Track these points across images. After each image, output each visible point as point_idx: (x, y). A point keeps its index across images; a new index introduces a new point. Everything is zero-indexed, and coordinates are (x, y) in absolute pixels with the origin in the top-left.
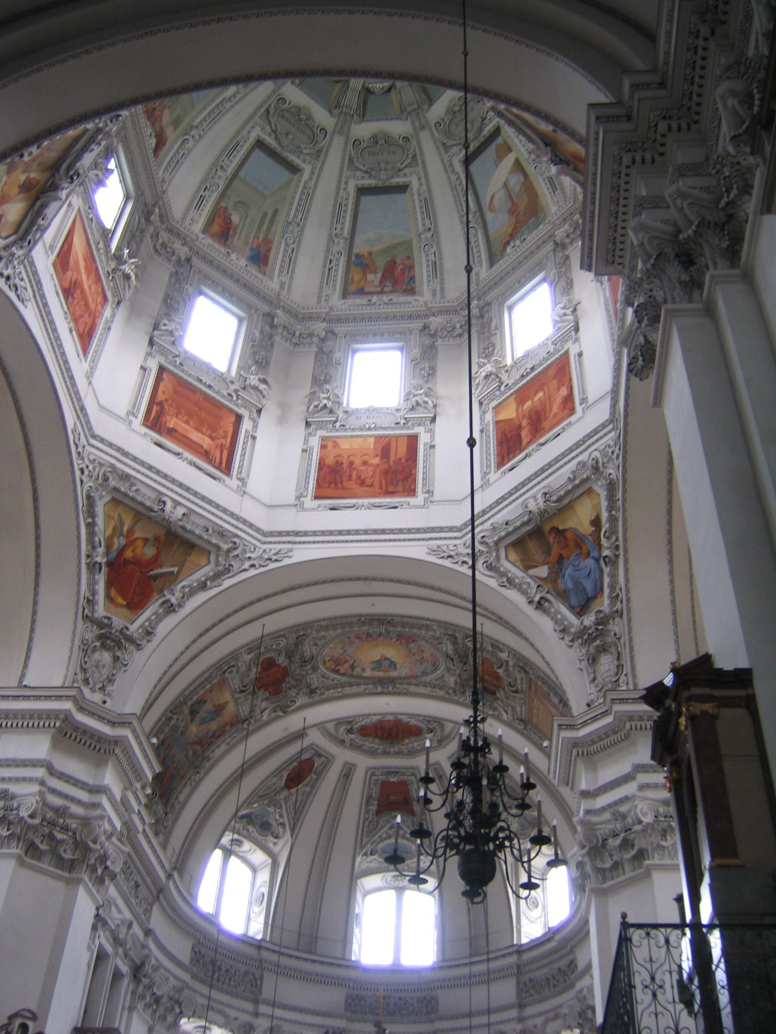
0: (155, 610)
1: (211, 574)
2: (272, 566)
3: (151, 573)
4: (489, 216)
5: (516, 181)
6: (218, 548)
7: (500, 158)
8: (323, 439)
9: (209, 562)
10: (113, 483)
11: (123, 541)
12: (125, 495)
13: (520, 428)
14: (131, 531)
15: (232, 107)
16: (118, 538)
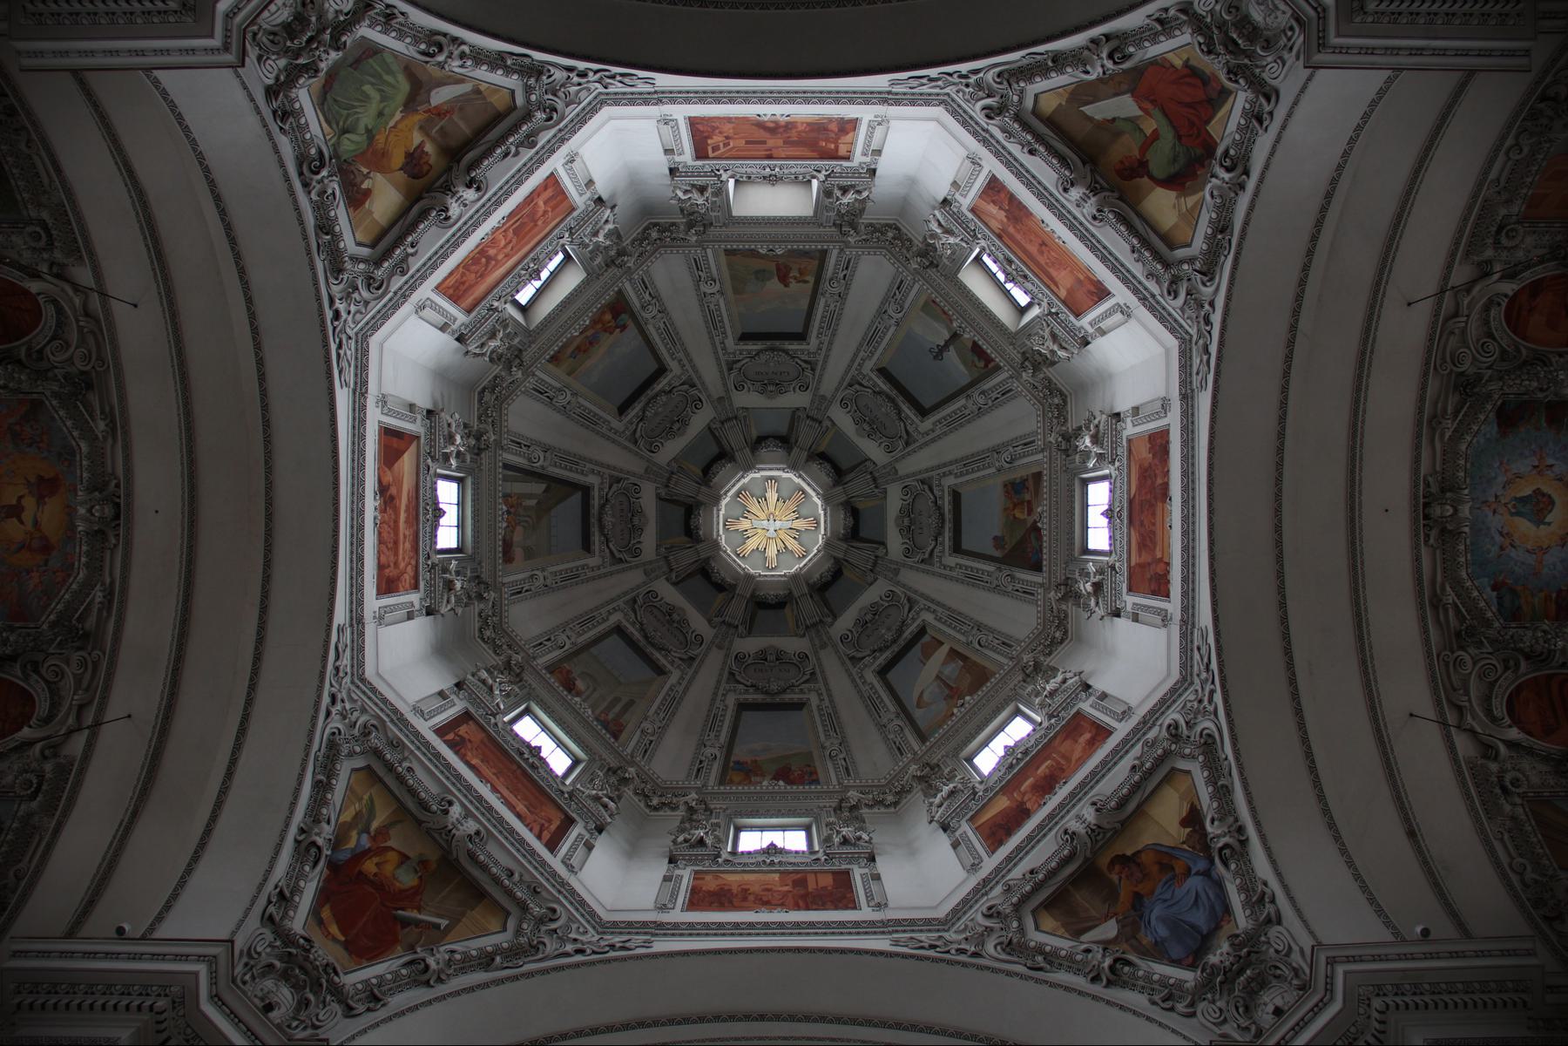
0: (394, 968)
1: (505, 945)
2: (612, 954)
3: (400, 912)
4: (918, 714)
5: (953, 670)
6: (523, 907)
7: (927, 654)
8: (696, 872)
9: (505, 929)
10: (375, 740)
11: (366, 842)
12: (390, 768)
13: (1022, 803)
14: (383, 832)
15: (594, 579)
16: (359, 834)
